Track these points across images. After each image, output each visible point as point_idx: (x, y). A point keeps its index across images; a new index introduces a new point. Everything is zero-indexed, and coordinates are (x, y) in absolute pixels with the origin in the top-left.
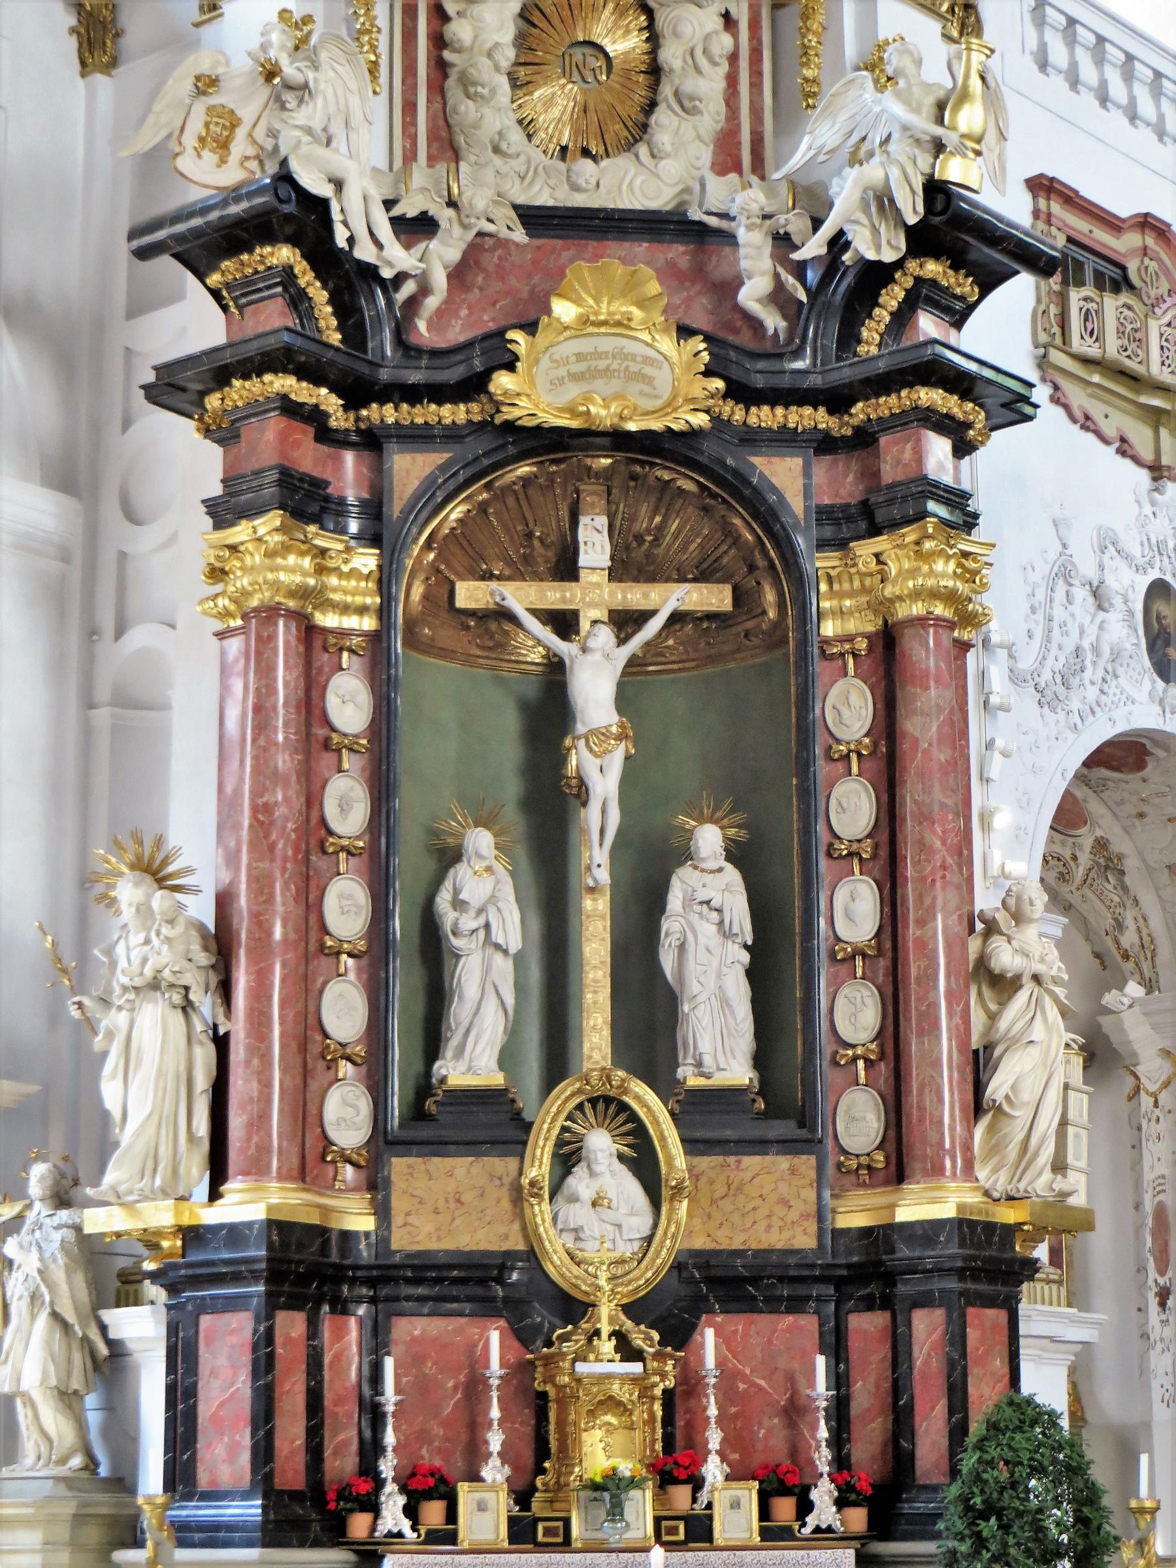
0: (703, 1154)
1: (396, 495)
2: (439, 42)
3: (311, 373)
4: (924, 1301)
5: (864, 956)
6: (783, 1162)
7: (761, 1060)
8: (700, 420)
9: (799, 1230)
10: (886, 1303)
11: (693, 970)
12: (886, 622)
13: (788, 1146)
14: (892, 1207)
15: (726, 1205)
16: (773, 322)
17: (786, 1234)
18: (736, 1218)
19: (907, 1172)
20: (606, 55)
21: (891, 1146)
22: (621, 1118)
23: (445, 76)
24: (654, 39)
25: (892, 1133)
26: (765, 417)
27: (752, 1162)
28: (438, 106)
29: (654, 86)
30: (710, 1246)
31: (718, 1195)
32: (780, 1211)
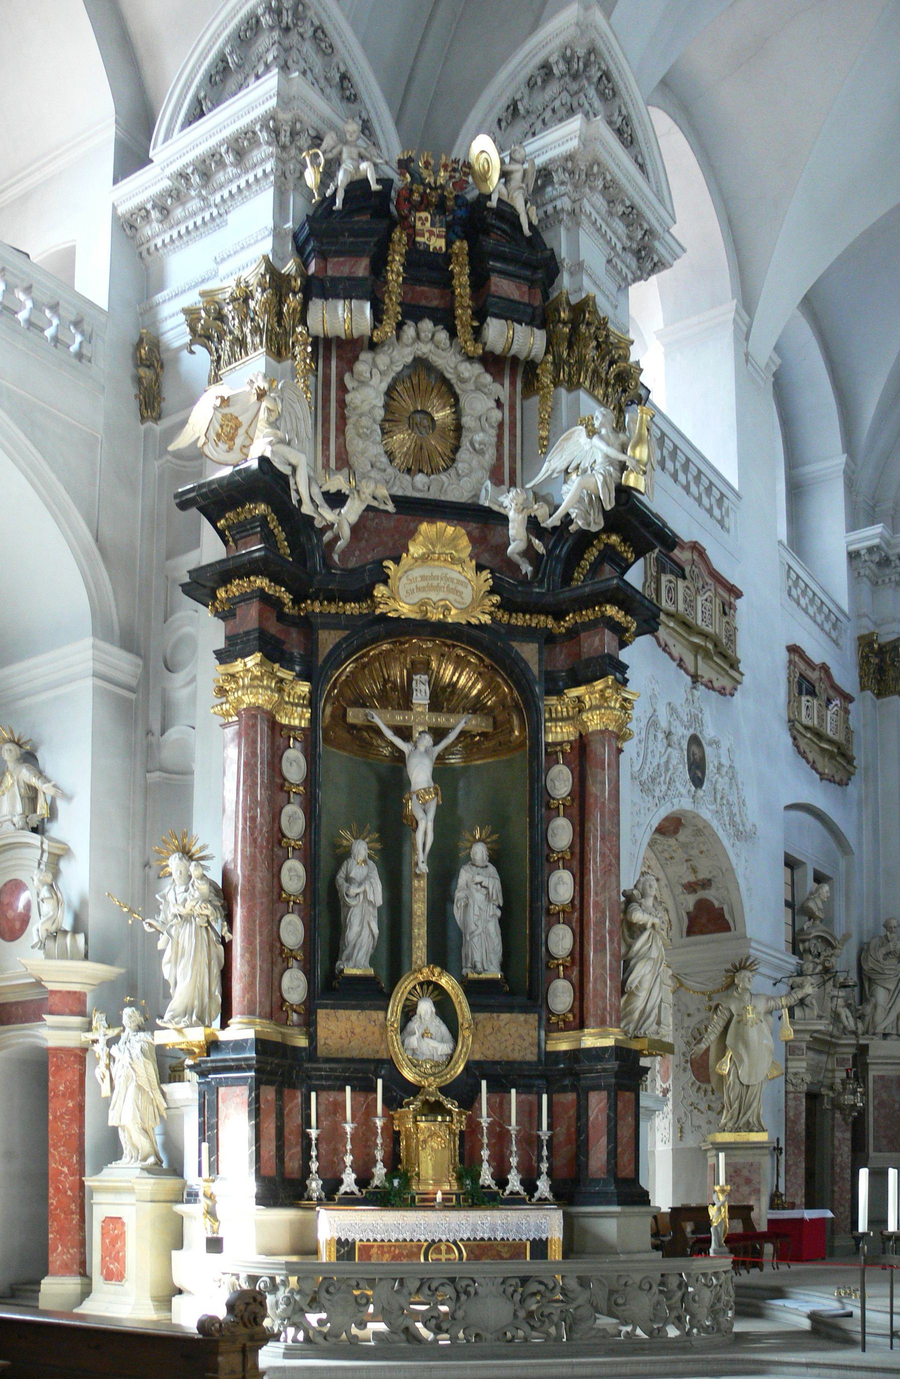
0: (479, 1012)
1: (321, 649)
2: (342, 404)
3: (275, 579)
4: (597, 1088)
5: (564, 911)
6: (522, 1017)
7: (504, 966)
8: (486, 619)
9: (528, 1051)
10: (574, 1088)
11: (472, 917)
12: (581, 735)
13: (525, 1010)
14: (579, 1040)
15: (491, 1038)
16: (527, 568)
17: (522, 1054)
18: (496, 1045)
19: (587, 1022)
20: (433, 419)
21: (577, 1011)
22: (436, 993)
23: (345, 424)
24: (458, 413)
25: (577, 1003)
26: (519, 620)
27: (505, 1017)
28: (341, 440)
29: (458, 437)
30: (483, 1058)
31: (487, 1033)
32: (518, 1041)
